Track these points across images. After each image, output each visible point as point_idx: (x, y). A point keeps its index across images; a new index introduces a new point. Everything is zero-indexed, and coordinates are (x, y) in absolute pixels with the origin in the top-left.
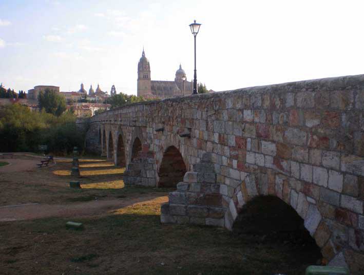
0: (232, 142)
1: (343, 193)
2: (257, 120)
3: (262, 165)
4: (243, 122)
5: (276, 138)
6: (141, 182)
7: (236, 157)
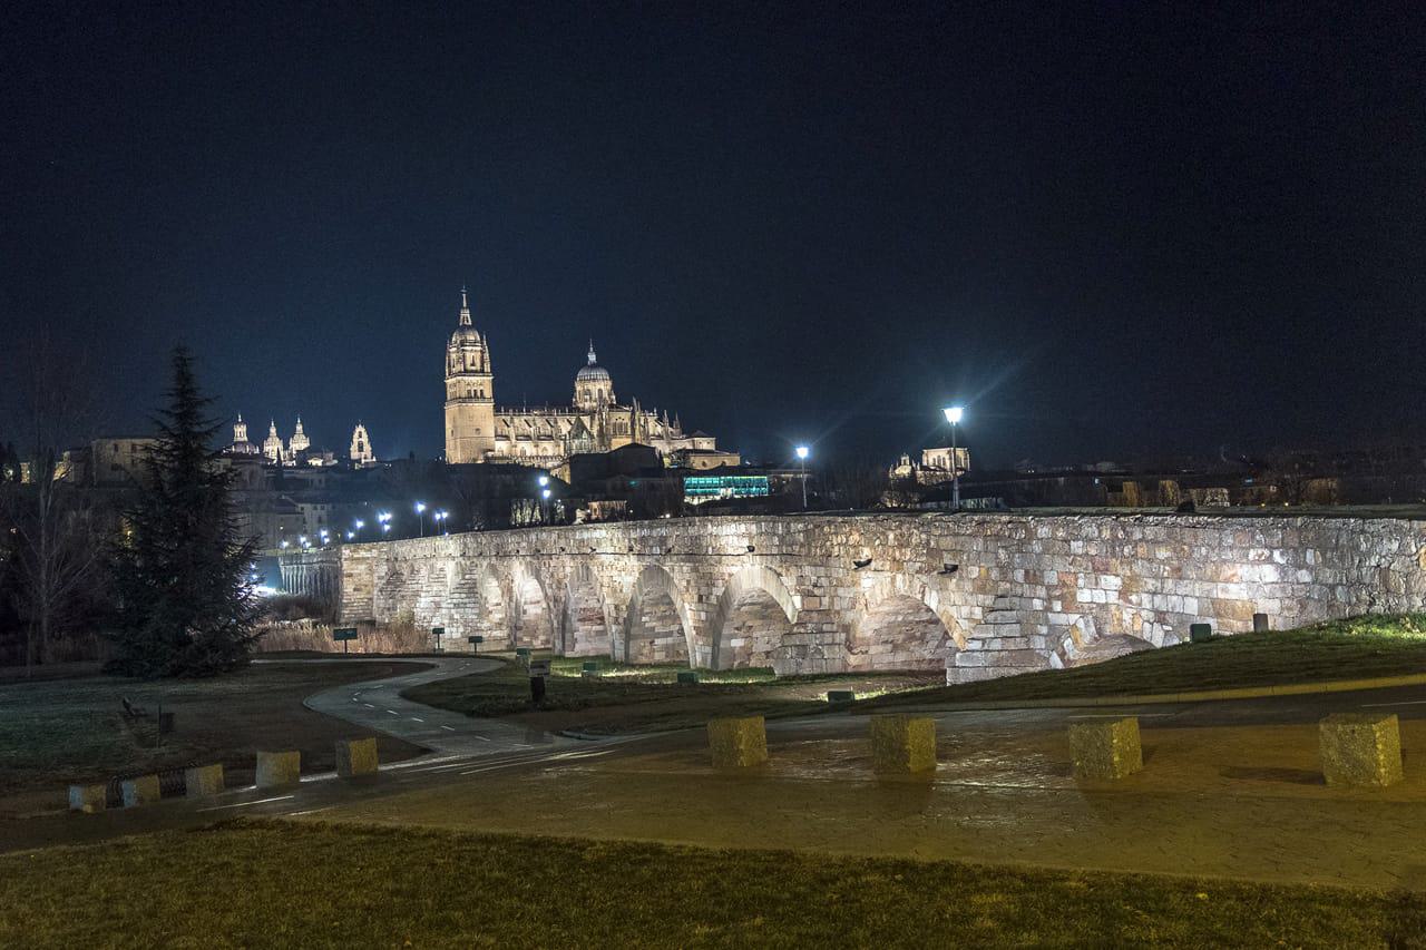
2: (1093, 552)
3: (1104, 601)
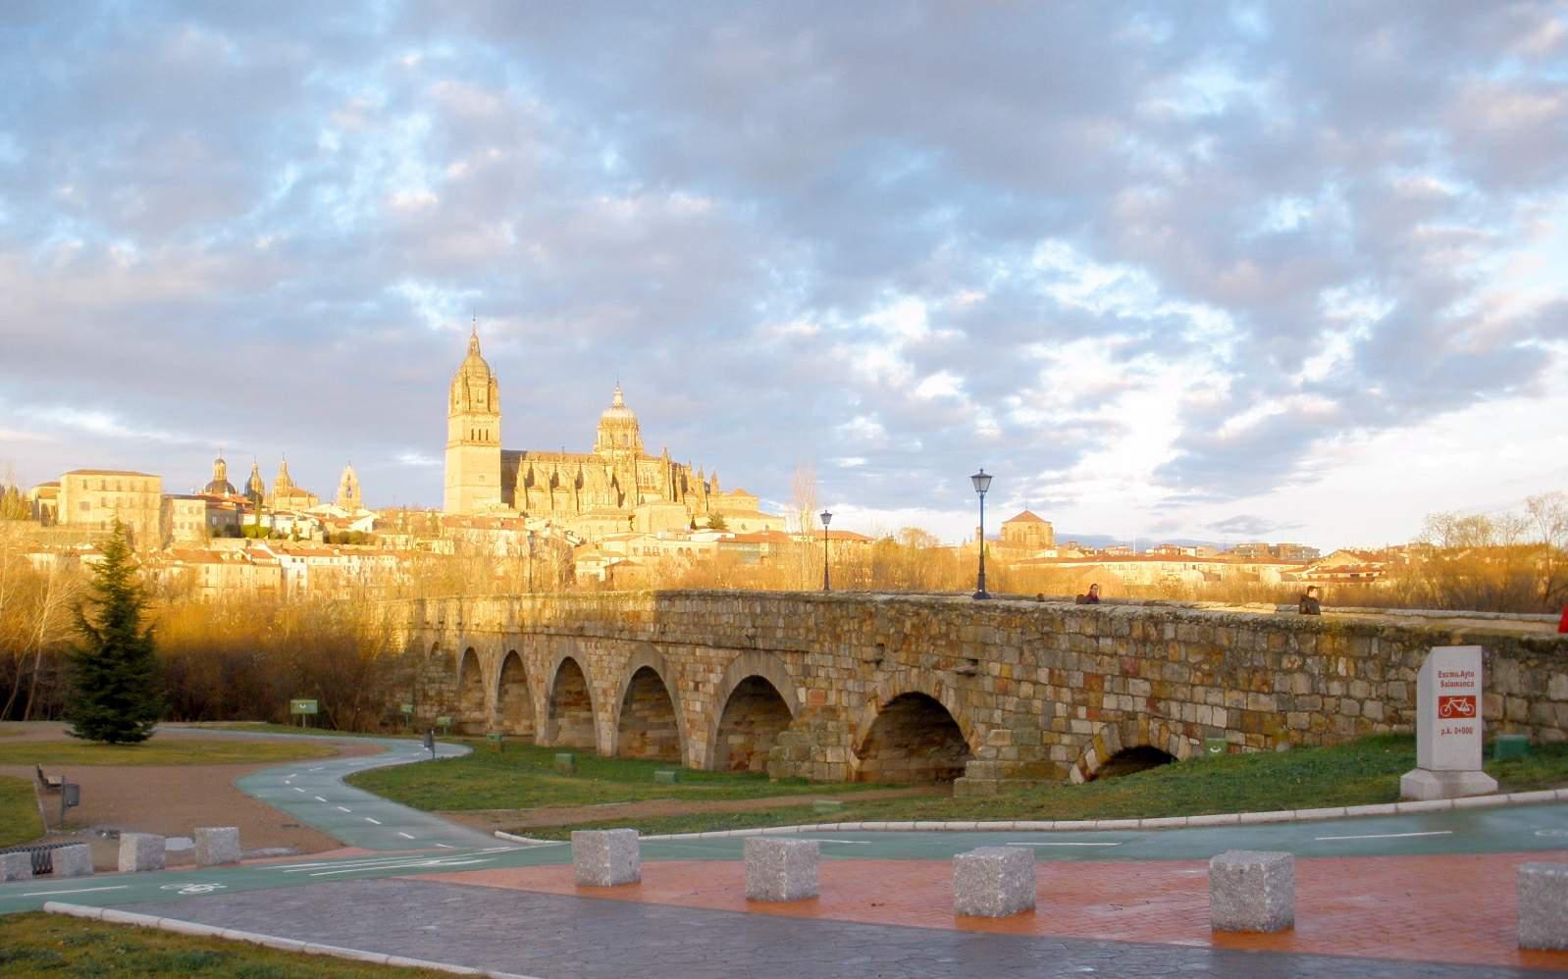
0: (1077, 680)
1: (1227, 728)
2: (1121, 651)
3: (1130, 709)
4: (1097, 652)
5: (1149, 675)
6: (812, 772)
7: (1085, 703)
